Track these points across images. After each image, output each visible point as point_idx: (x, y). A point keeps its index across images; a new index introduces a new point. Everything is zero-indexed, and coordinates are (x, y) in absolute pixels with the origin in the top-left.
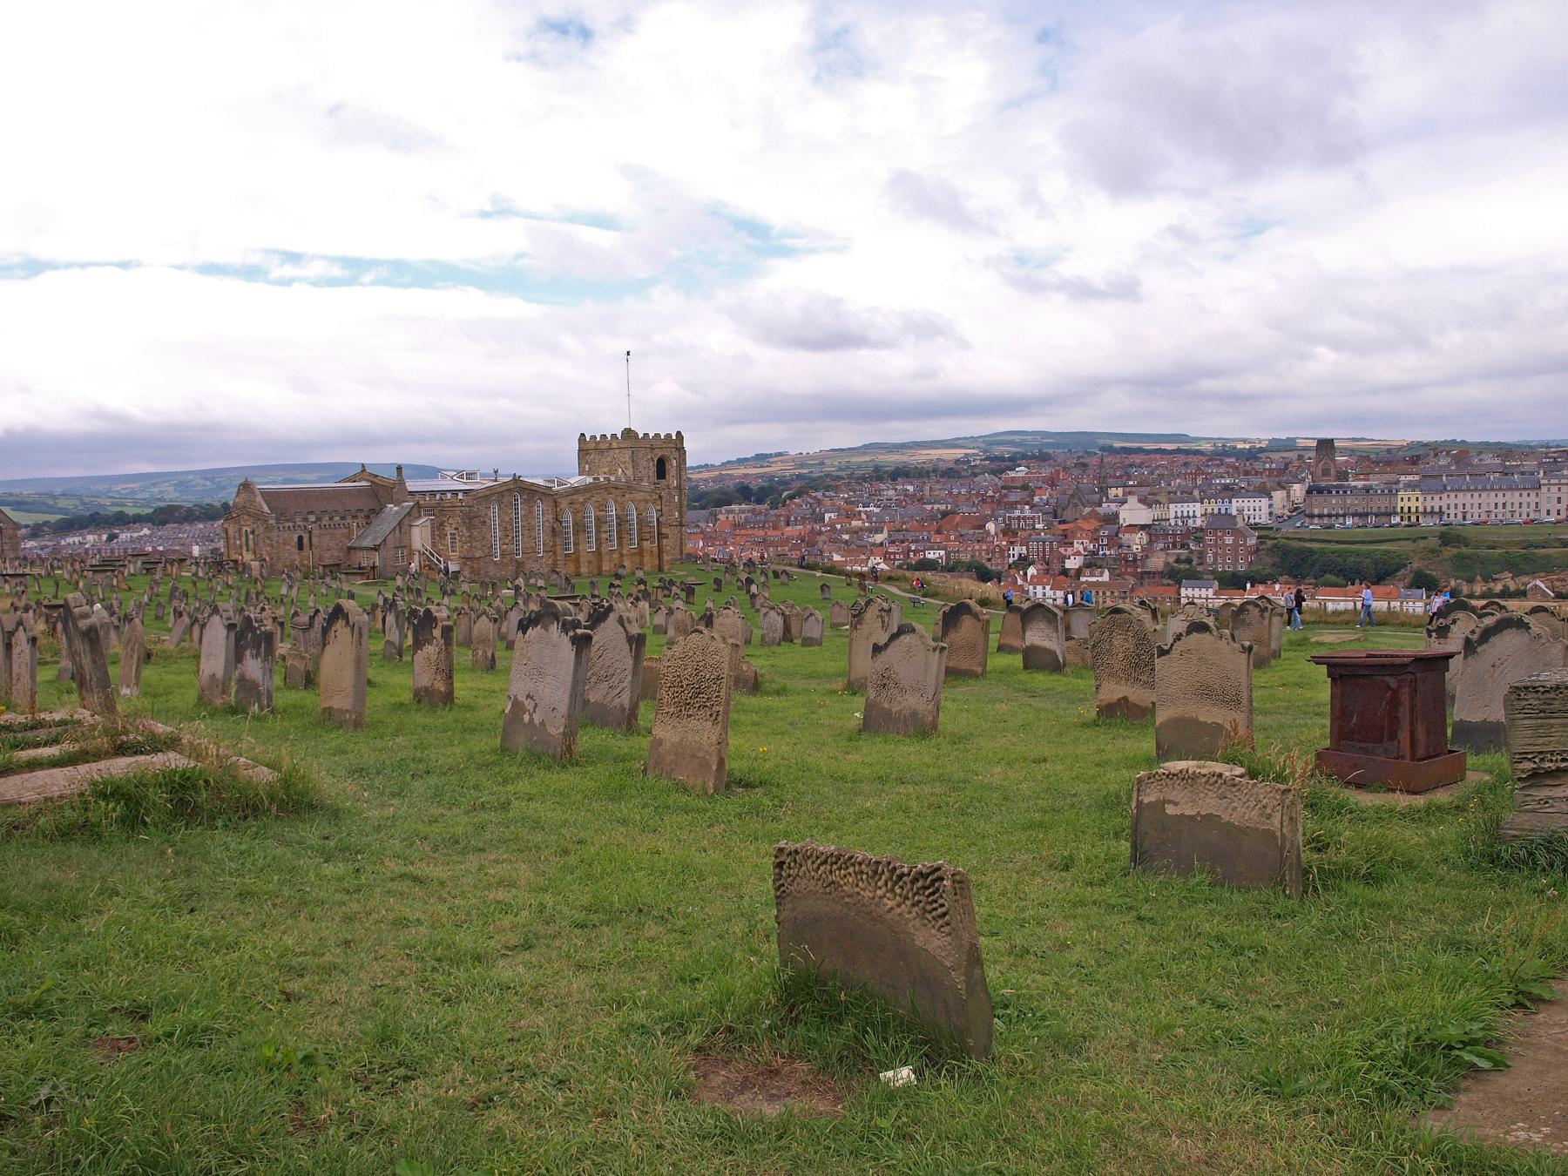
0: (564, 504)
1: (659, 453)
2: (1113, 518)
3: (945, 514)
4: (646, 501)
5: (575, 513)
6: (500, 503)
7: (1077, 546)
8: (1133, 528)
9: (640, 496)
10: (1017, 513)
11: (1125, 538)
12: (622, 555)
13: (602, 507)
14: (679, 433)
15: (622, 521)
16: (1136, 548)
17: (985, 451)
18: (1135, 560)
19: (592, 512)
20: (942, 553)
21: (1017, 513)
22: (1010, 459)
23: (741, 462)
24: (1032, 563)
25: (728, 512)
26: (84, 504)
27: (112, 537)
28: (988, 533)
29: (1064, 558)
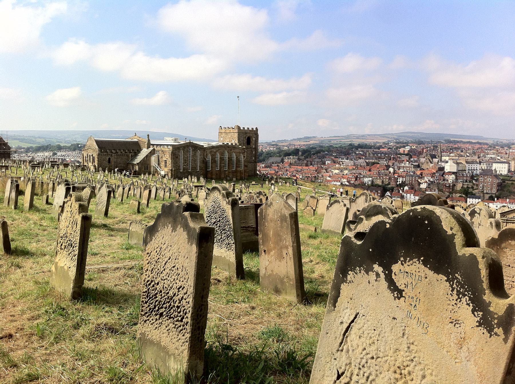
0: (208, 151)
1: (248, 135)
2: (442, 169)
3: (373, 163)
4: (240, 153)
5: (212, 156)
6: (184, 150)
7: (426, 179)
8: (450, 173)
9: (237, 150)
10: (403, 165)
11: (446, 177)
12: (229, 172)
13: (222, 154)
14: (257, 128)
15: (230, 159)
16: (450, 181)
17: (396, 139)
18: (450, 186)
19: (218, 155)
20: (371, 179)
21: (403, 165)
22: (406, 143)
23: (299, 139)
24: (407, 185)
25: (288, 158)
26: (46, 141)
27: (55, 154)
28: (390, 172)
29: (420, 184)
